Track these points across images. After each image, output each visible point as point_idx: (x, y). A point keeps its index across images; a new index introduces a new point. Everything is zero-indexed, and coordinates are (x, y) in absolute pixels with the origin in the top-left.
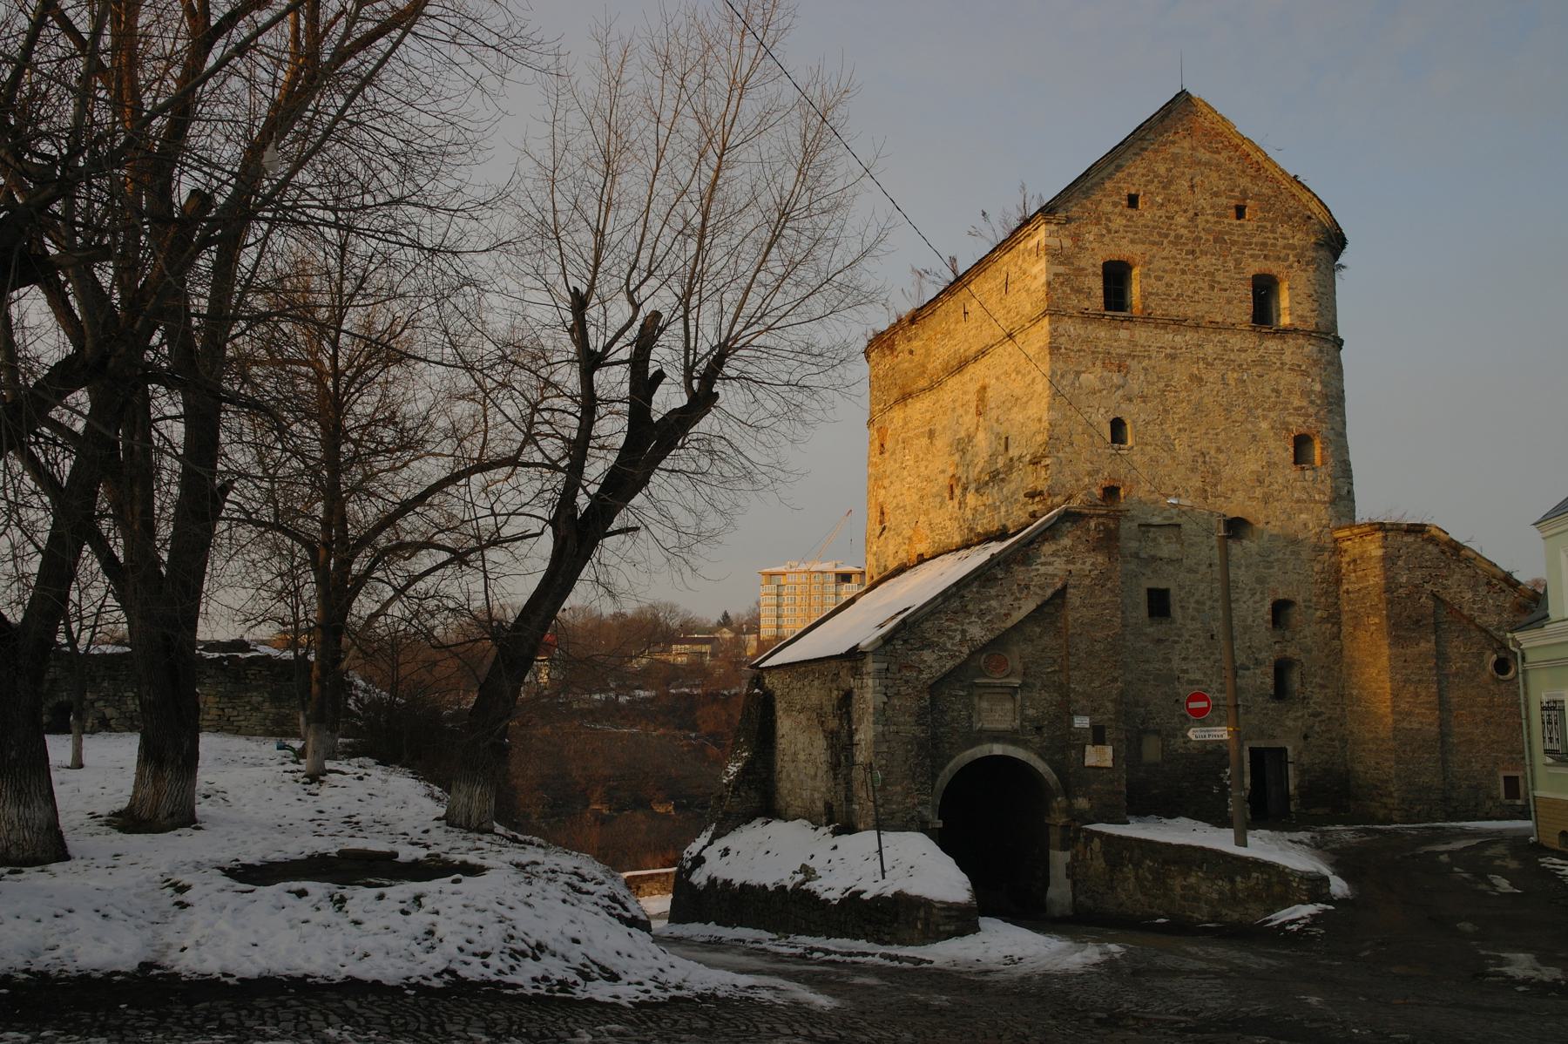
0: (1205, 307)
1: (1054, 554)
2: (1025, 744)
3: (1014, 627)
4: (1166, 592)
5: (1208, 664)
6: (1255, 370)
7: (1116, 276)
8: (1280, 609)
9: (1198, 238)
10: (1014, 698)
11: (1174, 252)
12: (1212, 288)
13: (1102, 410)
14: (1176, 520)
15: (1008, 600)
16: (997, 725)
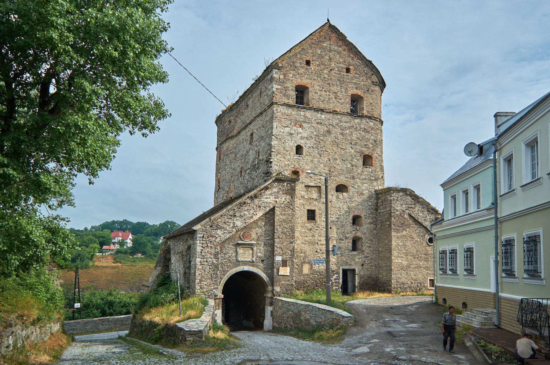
1: (271, 194)
2: (257, 266)
3: (254, 222)
7: (301, 92)
8: (356, 220)
12: (336, 98)
13: (293, 142)
14: (320, 185)
15: (252, 212)
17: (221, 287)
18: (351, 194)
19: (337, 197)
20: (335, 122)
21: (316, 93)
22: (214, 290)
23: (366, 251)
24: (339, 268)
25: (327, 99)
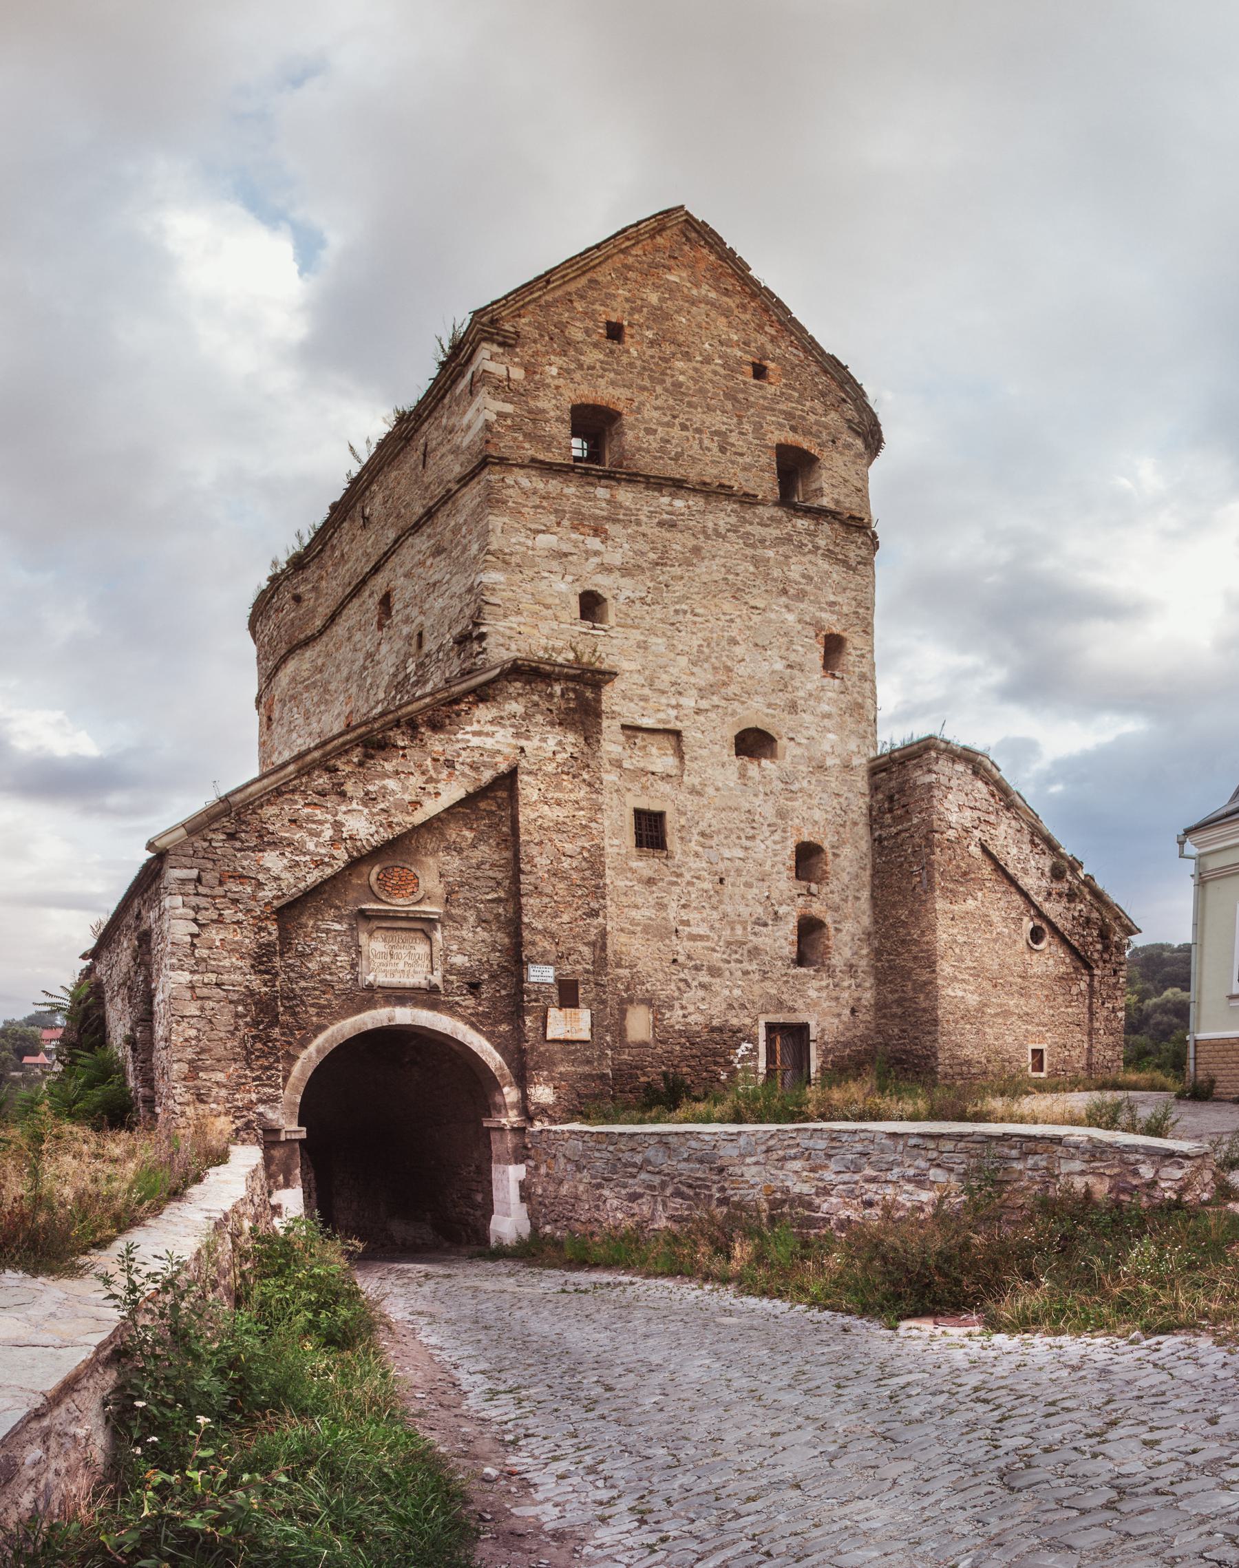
4: (659, 817)
8: (807, 859)
10: (429, 938)
11: (671, 402)
14: (678, 726)
18: (786, 763)
19: (743, 775)
21: (650, 431)
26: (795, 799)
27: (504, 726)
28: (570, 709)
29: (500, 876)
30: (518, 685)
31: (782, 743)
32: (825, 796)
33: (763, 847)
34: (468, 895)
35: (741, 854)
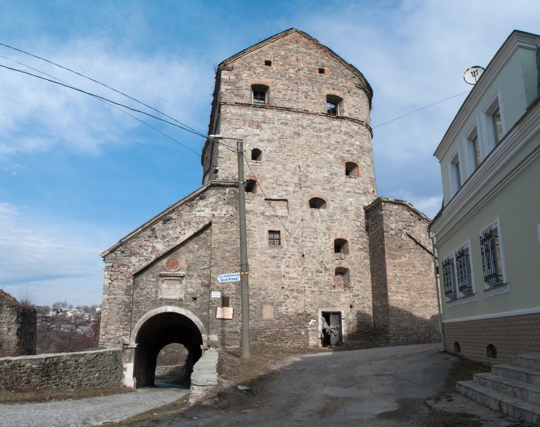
0: (303, 105)
2: (187, 307)
5: (300, 269)
6: (327, 133)
7: (260, 91)
8: (340, 245)
9: (300, 79)
11: (288, 83)
12: (306, 98)
14: (286, 198)
15: (178, 230)
16: (171, 296)
17: (135, 334)
19: (312, 214)
20: (305, 123)
22: (123, 337)
23: (356, 287)
24: (317, 311)
25: (295, 99)
26: (335, 223)
27: (208, 207)
28: (232, 198)
29: (206, 260)
30: (214, 191)
31: (328, 203)
32: (348, 221)
33: (321, 241)
34: (195, 267)
35: (311, 245)
